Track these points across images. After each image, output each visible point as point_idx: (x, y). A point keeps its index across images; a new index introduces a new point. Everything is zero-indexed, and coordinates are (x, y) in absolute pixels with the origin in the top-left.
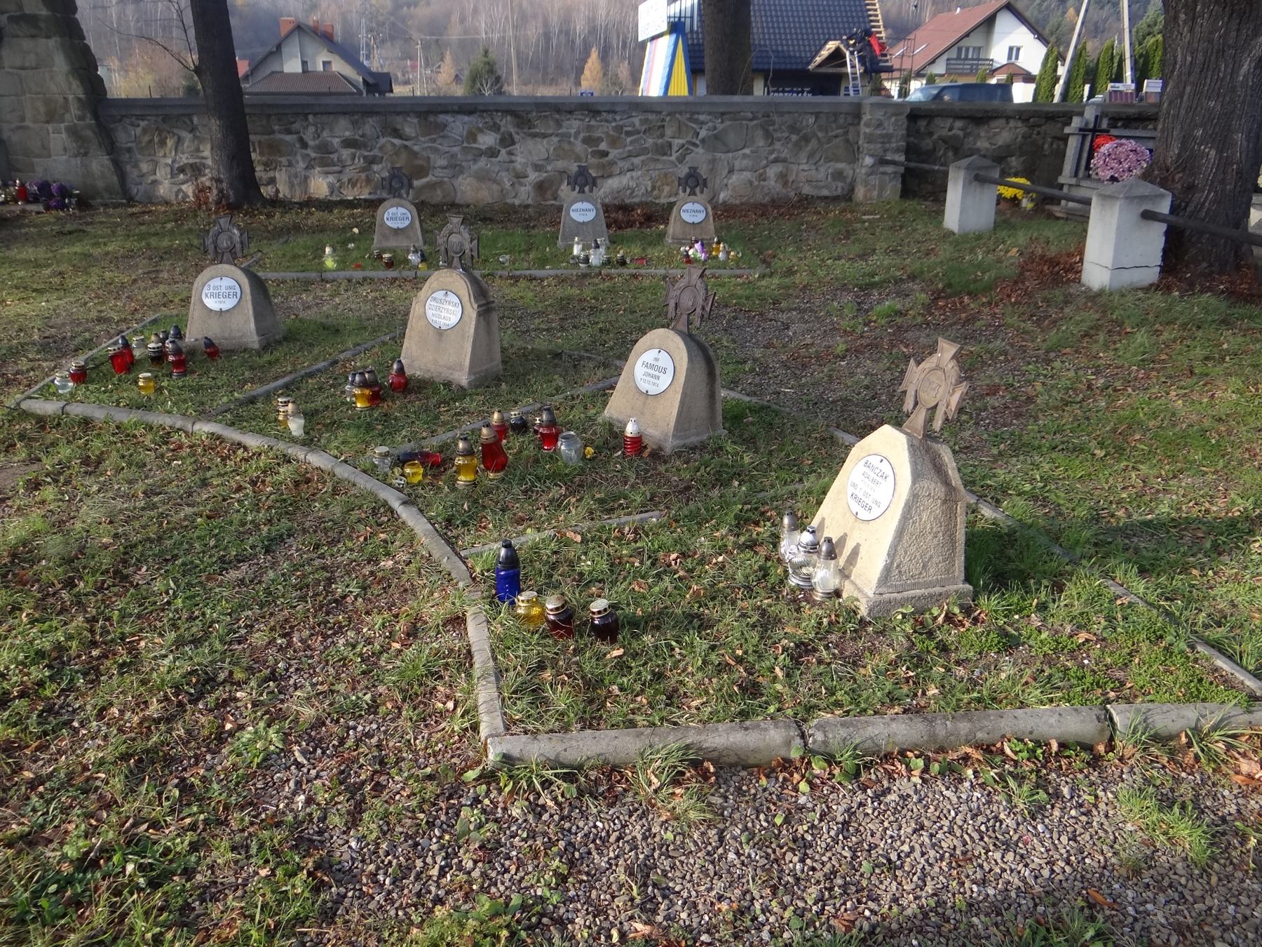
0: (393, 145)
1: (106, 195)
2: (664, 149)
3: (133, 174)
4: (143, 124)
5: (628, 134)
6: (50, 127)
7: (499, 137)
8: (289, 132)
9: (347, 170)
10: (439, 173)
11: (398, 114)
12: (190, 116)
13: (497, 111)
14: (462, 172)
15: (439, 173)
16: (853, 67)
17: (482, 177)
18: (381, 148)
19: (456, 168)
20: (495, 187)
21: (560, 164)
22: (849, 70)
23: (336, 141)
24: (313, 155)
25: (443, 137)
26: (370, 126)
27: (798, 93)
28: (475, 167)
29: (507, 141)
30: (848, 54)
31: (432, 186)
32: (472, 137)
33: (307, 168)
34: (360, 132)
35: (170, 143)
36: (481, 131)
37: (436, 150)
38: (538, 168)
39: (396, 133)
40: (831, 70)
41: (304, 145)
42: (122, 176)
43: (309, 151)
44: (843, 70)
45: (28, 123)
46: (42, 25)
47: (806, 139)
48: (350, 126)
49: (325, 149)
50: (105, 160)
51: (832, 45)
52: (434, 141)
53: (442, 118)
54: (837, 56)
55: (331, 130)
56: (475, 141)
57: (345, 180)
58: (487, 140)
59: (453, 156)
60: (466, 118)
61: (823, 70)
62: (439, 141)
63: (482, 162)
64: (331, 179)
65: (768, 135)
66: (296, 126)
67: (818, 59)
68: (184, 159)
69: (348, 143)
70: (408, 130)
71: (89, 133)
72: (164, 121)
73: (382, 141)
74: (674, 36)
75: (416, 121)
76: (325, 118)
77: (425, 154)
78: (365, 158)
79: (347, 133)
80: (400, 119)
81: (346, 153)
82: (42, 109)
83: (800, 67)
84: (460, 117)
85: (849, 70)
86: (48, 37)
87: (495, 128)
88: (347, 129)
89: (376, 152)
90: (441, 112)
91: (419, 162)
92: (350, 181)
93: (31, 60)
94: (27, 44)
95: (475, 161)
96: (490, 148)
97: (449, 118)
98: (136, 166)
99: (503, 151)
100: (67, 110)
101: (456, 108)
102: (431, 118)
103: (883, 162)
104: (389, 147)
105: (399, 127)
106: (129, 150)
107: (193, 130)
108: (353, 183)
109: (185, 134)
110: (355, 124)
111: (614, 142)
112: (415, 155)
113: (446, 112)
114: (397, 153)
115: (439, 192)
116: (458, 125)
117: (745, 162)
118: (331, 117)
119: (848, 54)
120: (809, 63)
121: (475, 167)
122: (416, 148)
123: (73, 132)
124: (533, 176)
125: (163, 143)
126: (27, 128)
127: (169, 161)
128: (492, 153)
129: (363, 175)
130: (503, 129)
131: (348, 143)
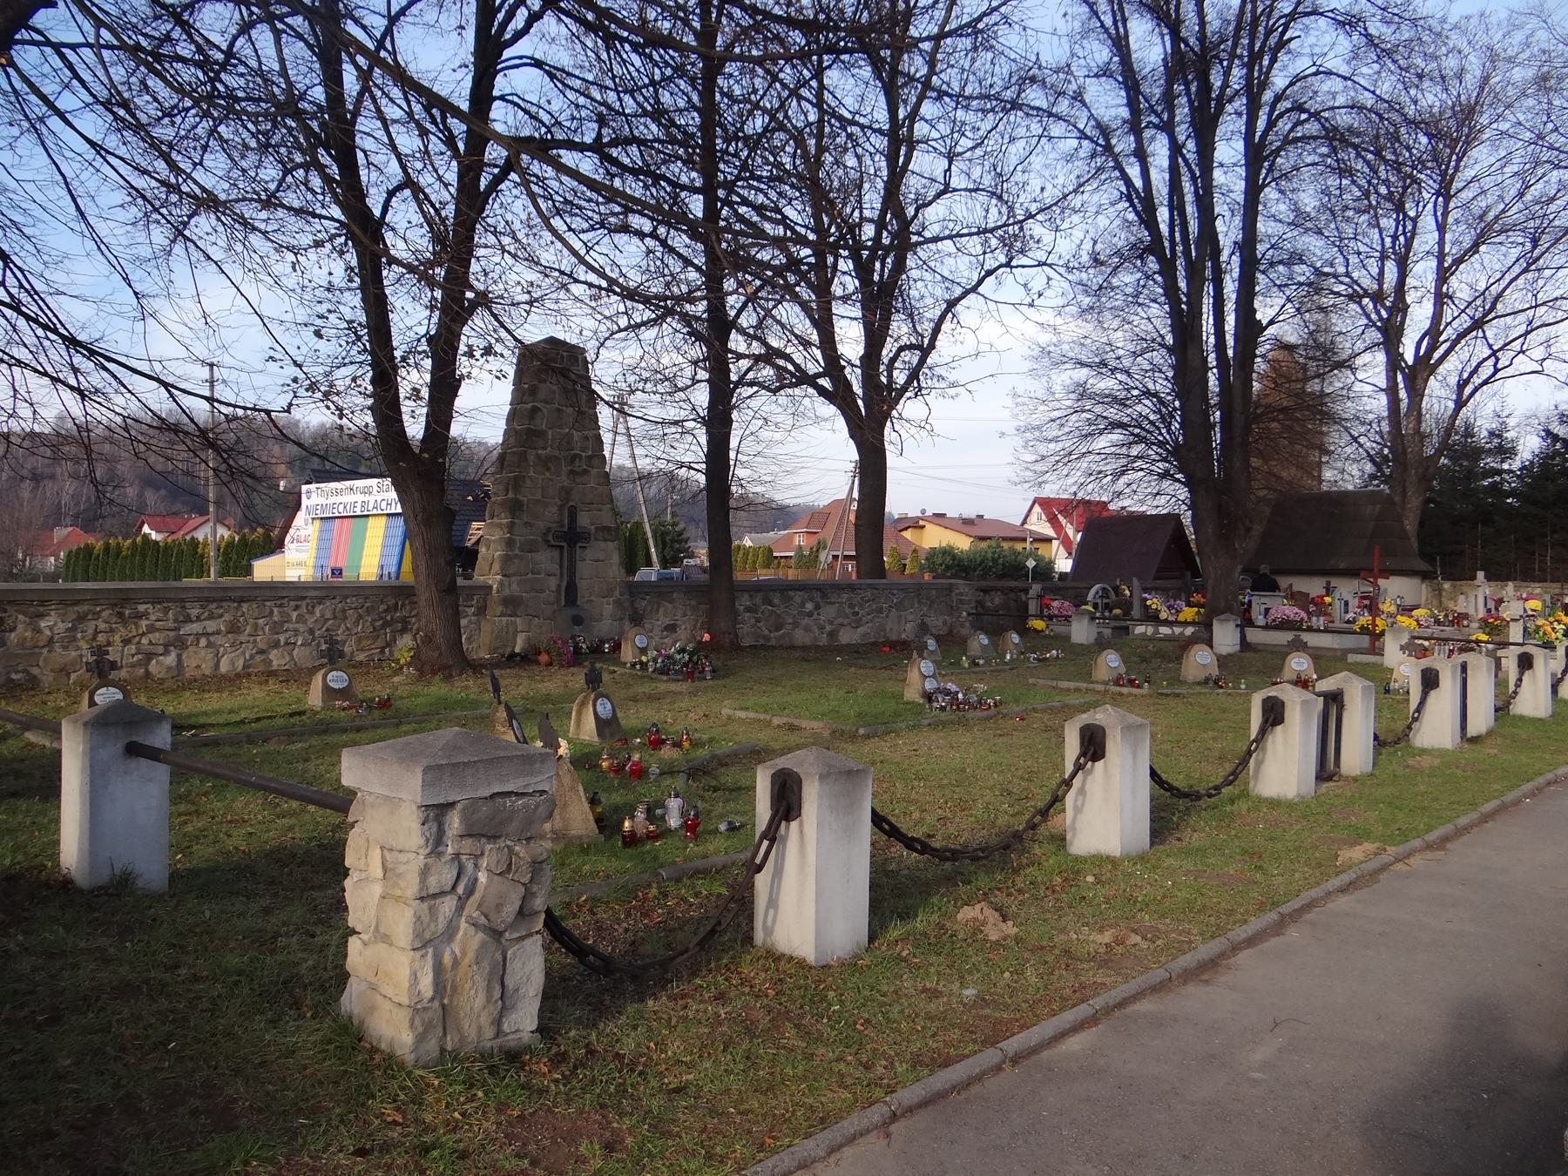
2: (880, 610)
5: (867, 601)
6: (605, 600)
19: (796, 624)
21: (840, 620)
29: (817, 607)
32: (803, 604)
35: (661, 610)
38: (831, 623)
39: (770, 603)
47: (933, 602)
58: (809, 606)
65: (919, 602)
69: (748, 610)
70: (776, 601)
87: (812, 599)
94: (603, 545)
103: (969, 614)
111: (862, 607)
116: (798, 597)
117: (912, 617)
123: (618, 603)
124: (828, 628)
128: (810, 614)
131: (748, 610)
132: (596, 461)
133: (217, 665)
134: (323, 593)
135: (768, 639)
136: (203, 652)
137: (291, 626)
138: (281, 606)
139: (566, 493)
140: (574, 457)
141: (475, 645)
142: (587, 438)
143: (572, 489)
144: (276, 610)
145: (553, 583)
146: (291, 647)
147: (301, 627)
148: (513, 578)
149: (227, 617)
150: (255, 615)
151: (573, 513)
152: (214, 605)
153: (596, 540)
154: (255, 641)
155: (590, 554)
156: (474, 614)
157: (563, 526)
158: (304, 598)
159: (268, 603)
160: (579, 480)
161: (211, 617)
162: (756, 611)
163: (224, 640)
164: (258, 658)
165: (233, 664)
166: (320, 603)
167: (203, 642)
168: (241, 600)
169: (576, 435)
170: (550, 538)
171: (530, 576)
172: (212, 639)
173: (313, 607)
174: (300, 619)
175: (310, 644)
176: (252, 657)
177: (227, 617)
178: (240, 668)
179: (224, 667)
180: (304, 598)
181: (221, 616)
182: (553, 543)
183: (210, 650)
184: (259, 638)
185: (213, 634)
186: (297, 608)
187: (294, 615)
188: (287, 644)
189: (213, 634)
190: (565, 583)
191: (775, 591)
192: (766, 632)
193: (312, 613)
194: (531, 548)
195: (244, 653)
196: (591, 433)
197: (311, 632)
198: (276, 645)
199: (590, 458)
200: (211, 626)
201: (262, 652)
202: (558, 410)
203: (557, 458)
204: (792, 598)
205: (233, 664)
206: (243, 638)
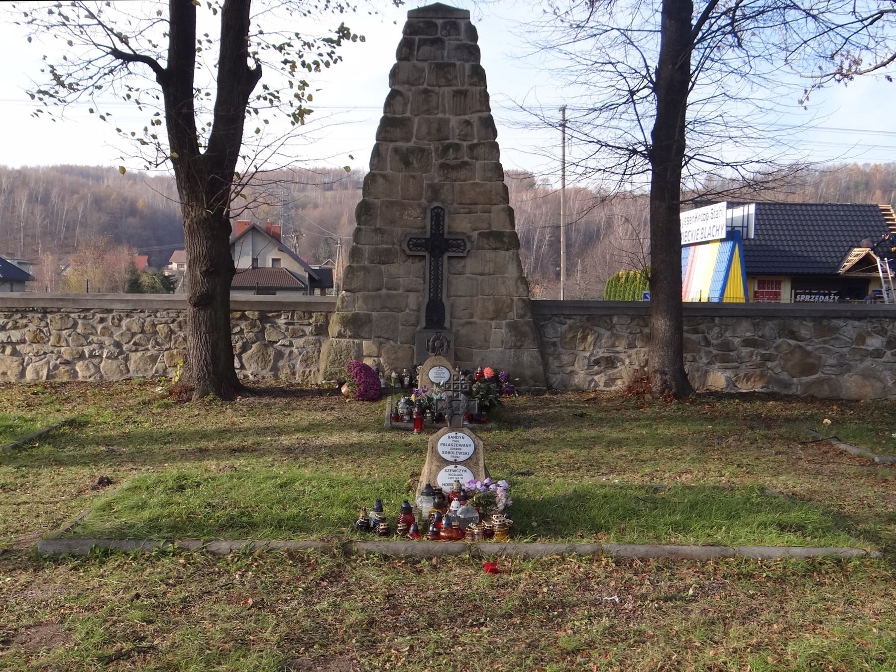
0: (789, 345)
1: (531, 382)
3: (554, 364)
4: (569, 322)
6: (493, 323)
7: (885, 339)
8: (696, 332)
9: (743, 366)
10: (828, 371)
11: (796, 318)
12: (611, 317)
13: (886, 317)
14: (849, 371)
15: (828, 371)
16: (884, 271)
17: (868, 375)
18: (777, 348)
19: (844, 367)
20: (878, 385)
22: (881, 274)
23: (737, 341)
24: (715, 352)
25: (836, 339)
26: (769, 329)
27: (825, 295)
28: (861, 366)
30: (878, 259)
31: (820, 382)
32: (861, 339)
33: (709, 363)
34: (760, 333)
35: (590, 339)
36: (869, 334)
37: (828, 351)
39: (793, 335)
40: (861, 275)
41: (708, 344)
42: (546, 365)
43: (711, 349)
44: (874, 274)
45: (475, 319)
46: (506, 240)
48: (752, 328)
49: (726, 347)
50: (535, 351)
51: (857, 254)
52: (825, 342)
53: (835, 322)
54: (866, 263)
55: (734, 331)
56: (863, 343)
57: (742, 375)
58: (874, 342)
59: (842, 356)
60: (857, 323)
61: (853, 274)
62: (832, 342)
63: (868, 362)
64: (729, 373)
66: (702, 327)
67: (848, 265)
68: (601, 353)
69: (747, 343)
70: (804, 332)
71: (527, 329)
72: (588, 320)
73: (779, 341)
74: (729, 245)
75: (811, 324)
76: (729, 321)
77: (817, 353)
78: (762, 355)
79: (748, 334)
80: (796, 322)
81: (745, 351)
82: (491, 308)
83: (829, 271)
84: (850, 322)
85: (881, 274)
86: (507, 250)
87: (882, 332)
88: (748, 331)
89: (772, 351)
90: (835, 318)
91: (811, 361)
92: (746, 375)
93: (490, 268)
94: (490, 254)
95: (862, 360)
96: (877, 350)
97: (841, 323)
98: (558, 357)
99: (889, 353)
100: (510, 307)
101: (849, 314)
102: (825, 323)
104: (785, 347)
105: (795, 329)
106: (554, 344)
107: (611, 328)
108: (748, 378)
109: (602, 331)
110: (756, 326)
112: (809, 354)
113: (839, 318)
114: (792, 352)
115: (826, 387)
118: (735, 320)
119: (878, 259)
120: (838, 268)
121: (861, 366)
122: (809, 348)
123: (513, 328)
125: (584, 338)
126: (475, 323)
127: (588, 354)
128: (878, 354)
129: (758, 371)
130: (889, 333)
131: (747, 343)
132: (481, 151)
133: (22, 374)
134: (130, 307)
135: (787, 385)
136: (8, 361)
137: (95, 339)
138: (85, 318)
139: (435, 191)
140: (446, 149)
141: (314, 369)
142: (468, 123)
143: (442, 186)
144: (80, 321)
145: (412, 300)
146: (97, 360)
147: (107, 341)
148: (359, 294)
149: (32, 327)
150: (58, 326)
151: (438, 217)
152: (19, 315)
153: (479, 248)
154: (59, 352)
155: (471, 265)
156: (311, 333)
157: (425, 232)
158: (111, 311)
159: (72, 315)
160: (453, 174)
161: (15, 327)
162: (763, 345)
163: (29, 349)
164: (62, 369)
165: (37, 373)
166: (127, 316)
167: (8, 350)
168: (45, 312)
169: (454, 121)
170: (405, 246)
171: (384, 291)
172: (18, 347)
173: (120, 320)
174: (106, 331)
175: (116, 358)
176: (56, 367)
177: (32, 327)
178: (44, 378)
179: (29, 375)
180: (111, 311)
181: (26, 326)
182: (408, 252)
183: (15, 358)
184: (62, 349)
185: (18, 343)
186: (102, 320)
187: (100, 327)
188: (92, 356)
189: (18, 343)
190: (427, 300)
191: (803, 318)
192: (785, 376)
193: (119, 326)
194: (384, 257)
195: (48, 363)
196: (474, 118)
197: (118, 345)
198: (82, 356)
199: (472, 148)
200: (15, 335)
201: (67, 363)
202: (426, 92)
203: (422, 150)
204: (838, 329)
205: (37, 373)
206: (48, 348)
